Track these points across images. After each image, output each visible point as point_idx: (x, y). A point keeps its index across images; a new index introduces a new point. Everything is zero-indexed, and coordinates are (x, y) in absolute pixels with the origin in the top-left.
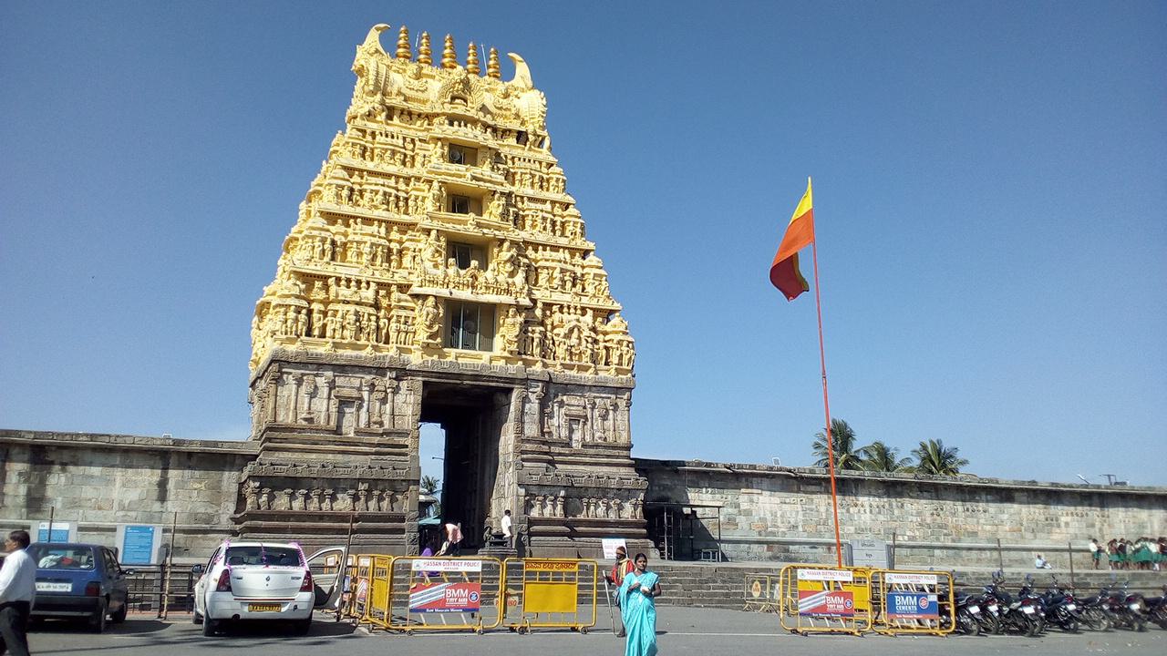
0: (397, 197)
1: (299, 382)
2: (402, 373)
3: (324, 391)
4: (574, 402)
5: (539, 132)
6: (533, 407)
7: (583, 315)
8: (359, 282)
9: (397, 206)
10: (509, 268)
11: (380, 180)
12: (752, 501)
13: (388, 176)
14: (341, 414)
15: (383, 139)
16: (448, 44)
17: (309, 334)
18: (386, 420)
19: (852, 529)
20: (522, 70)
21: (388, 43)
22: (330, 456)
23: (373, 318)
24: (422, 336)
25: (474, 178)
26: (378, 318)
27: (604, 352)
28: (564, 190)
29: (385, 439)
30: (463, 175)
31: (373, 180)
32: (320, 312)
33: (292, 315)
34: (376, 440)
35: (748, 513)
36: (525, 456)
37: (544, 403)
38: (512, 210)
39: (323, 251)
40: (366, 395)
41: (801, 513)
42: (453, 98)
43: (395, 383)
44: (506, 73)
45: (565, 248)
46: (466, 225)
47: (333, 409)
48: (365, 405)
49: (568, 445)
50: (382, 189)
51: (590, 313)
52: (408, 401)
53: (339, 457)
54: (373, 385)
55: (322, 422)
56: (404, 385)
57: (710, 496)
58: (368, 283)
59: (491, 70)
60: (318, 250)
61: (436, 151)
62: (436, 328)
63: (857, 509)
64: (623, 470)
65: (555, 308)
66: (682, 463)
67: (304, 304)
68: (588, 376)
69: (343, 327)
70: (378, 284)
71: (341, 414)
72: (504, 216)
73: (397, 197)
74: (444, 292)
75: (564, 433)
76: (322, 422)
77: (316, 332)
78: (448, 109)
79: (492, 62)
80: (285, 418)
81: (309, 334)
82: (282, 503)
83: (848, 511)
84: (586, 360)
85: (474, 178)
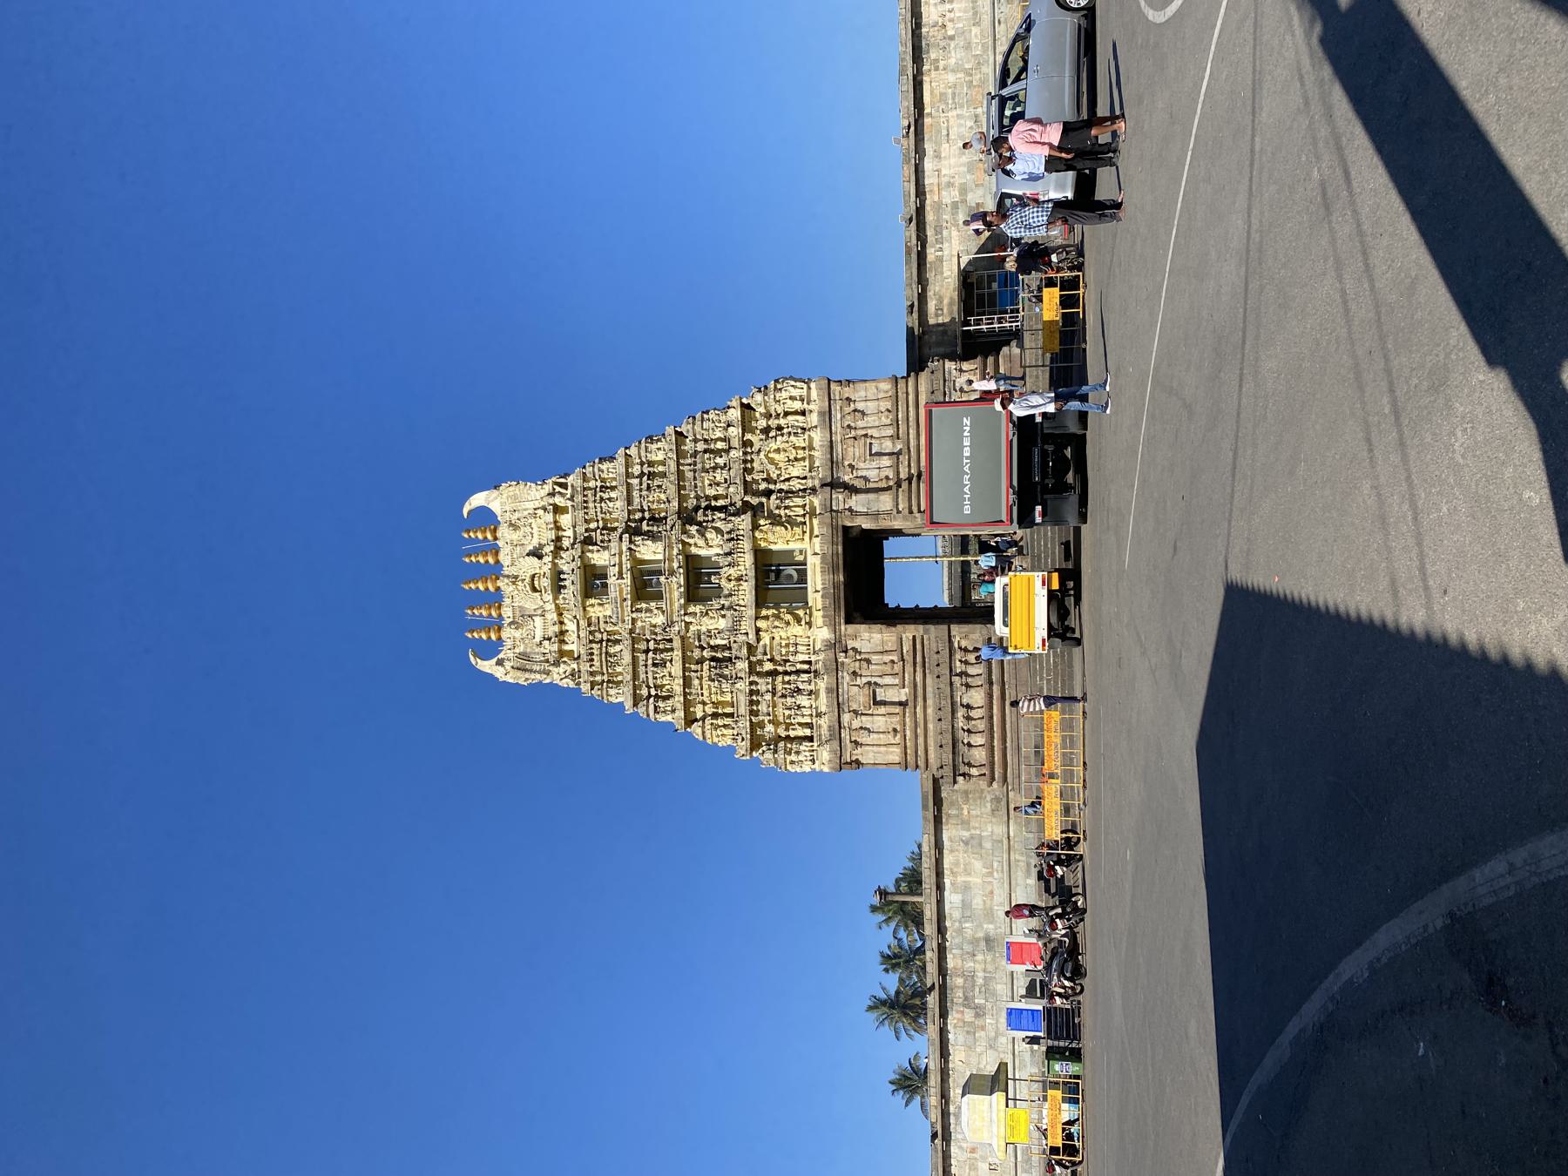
0: (655, 651)
1: (856, 743)
2: (837, 646)
3: (866, 721)
4: (852, 452)
5: (548, 488)
6: (857, 502)
7: (751, 444)
8: (752, 692)
9: (667, 650)
10: (711, 535)
11: (642, 669)
12: (950, 185)
13: (634, 657)
14: (884, 703)
15: (597, 663)
16: (473, 586)
17: (811, 739)
18: (887, 658)
19: (975, 30)
20: (478, 500)
21: (490, 650)
22: (930, 711)
23: (787, 678)
24: (797, 630)
25: (621, 576)
26: (786, 673)
27: (790, 418)
28: (612, 459)
29: (909, 658)
30: (619, 585)
31: (642, 676)
32: (787, 729)
33: (793, 757)
34: (909, 668)
35: (964, 190)
36: (915, 509)
37: (853, 490)
38: (645, 527)
39: (725, 726)
40: (865, 680)
41: (959, 111)
42: (534, 590)
43: (851, 653)
44: (485, 518)
45: (678, 464)
46: (674, 587)
47: (882, 710)
48: (873, 680)
49: (899, 453)
50: (651, 668)
51: (748, 436)
52: (870, 638)
53: (930, 702)
54: (854, 673)
55: (897, 719)
56: (851, 644)
57: (946, 245)
58: (751, 683)
59: (489, 536)
60: (725, 731)
61: (597, 610)
62: (788, 617)
63: (950, 25)
64: (923, 388)
65: (749, 478)
66: (910, 331)
67: (781, 744)
68: (818, 437)
69: (799, 707)
70: (750, 673)
71: (884, 703)
72: (653, 537)
73: (655, 651)
74: (751, 612)
75: (886, 461)
76: (896, 719)
77: (808, 732)
78: (549, 597)
79: (480, 536)
80: (895, 755)
81: (811, 739)
82: (979, 755)
83: (952, 38)
84: (800, 441)
85: (621, 576)
